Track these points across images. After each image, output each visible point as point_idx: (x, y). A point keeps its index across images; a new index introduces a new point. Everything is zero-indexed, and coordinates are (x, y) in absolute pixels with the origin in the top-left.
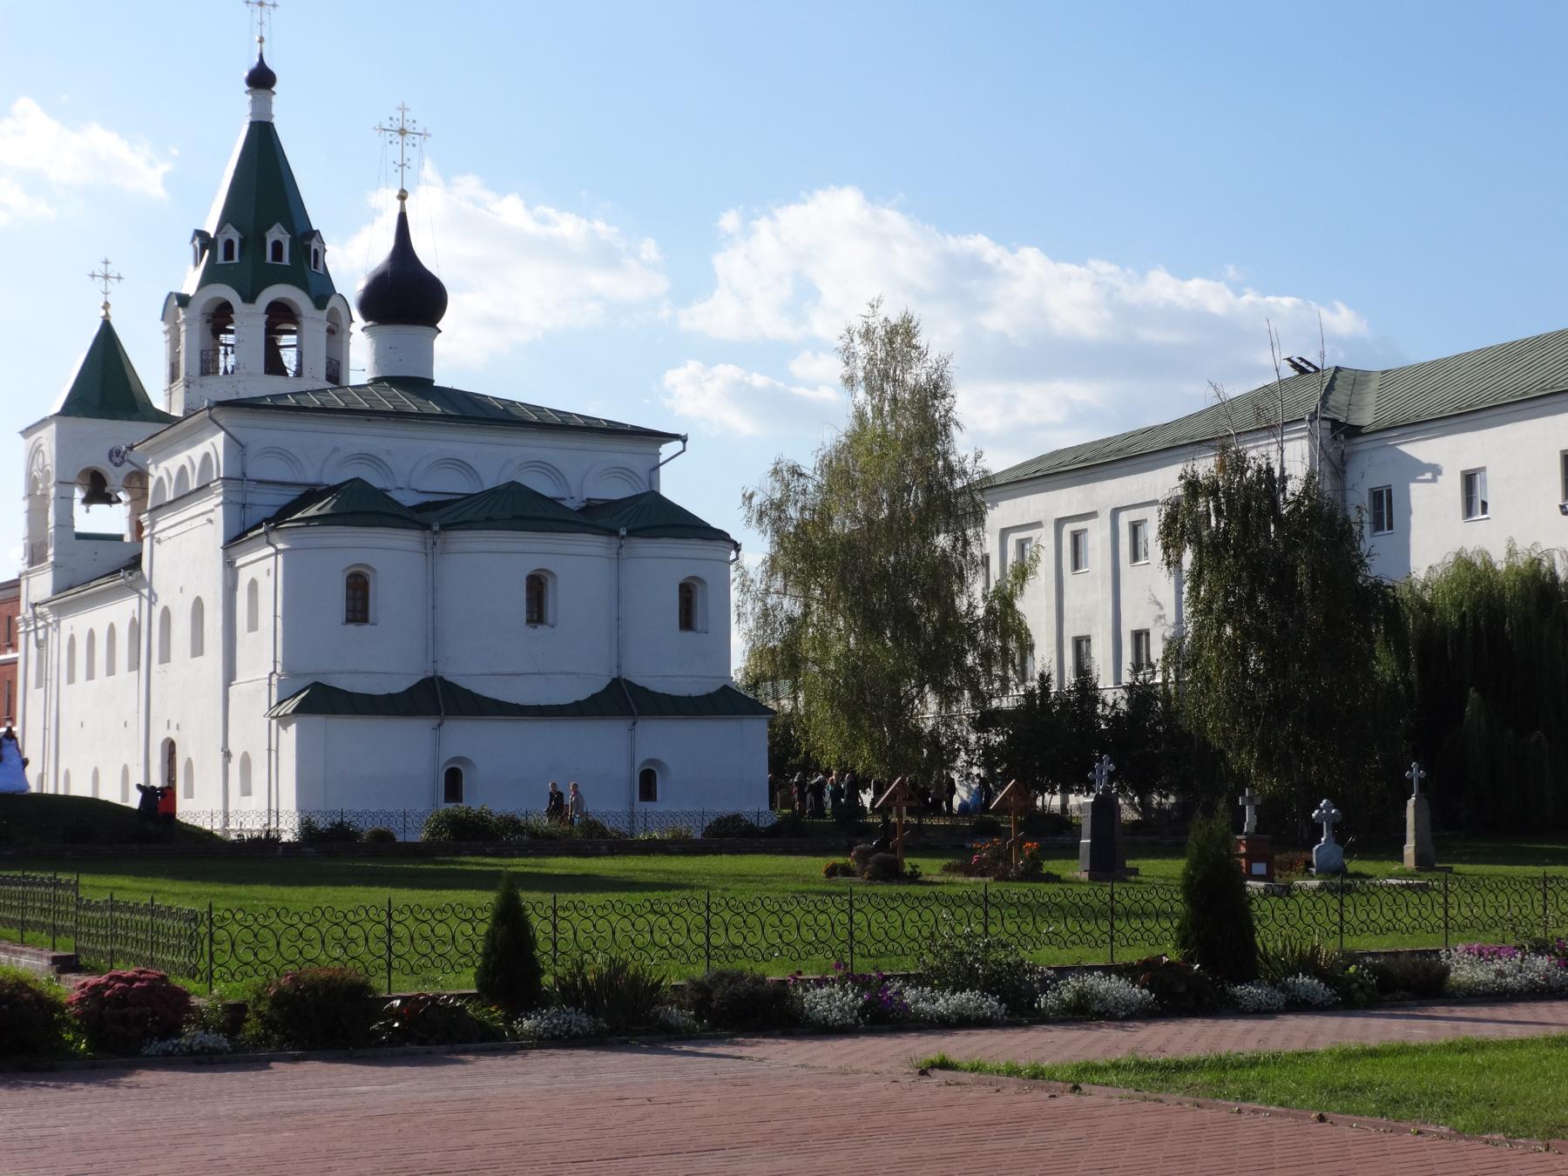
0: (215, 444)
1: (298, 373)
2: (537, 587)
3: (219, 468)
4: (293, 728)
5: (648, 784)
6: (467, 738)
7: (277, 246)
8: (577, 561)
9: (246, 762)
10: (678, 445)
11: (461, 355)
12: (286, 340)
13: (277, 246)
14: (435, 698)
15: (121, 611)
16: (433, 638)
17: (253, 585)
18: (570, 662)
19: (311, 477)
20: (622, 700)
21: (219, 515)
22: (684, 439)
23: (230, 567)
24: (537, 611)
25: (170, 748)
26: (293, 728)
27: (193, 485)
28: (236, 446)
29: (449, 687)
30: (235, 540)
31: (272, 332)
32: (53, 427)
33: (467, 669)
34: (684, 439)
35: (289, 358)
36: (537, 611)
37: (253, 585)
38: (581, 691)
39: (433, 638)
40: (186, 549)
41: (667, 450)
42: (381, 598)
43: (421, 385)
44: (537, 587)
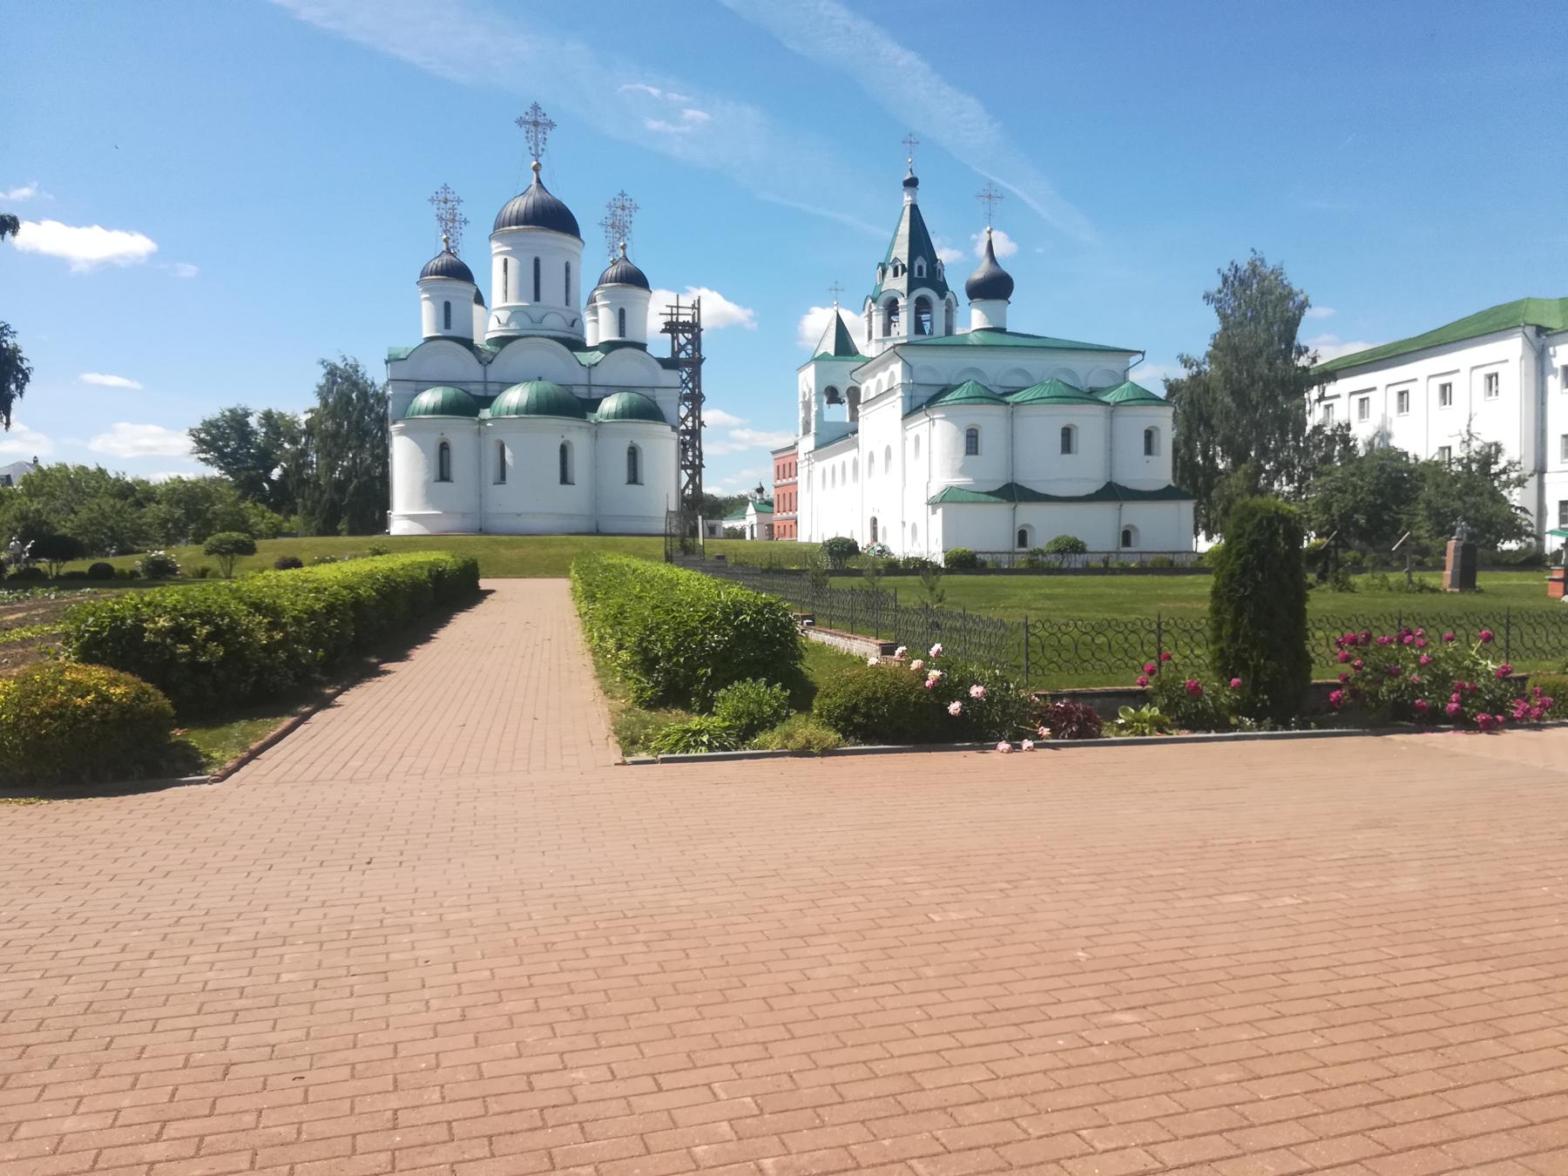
0: (897, 368)
1: (931, 333)
2: (1067, 433)
3: (899, 379)
4: (940, 511)
5: (1126, 537)
6: (1029, 514)
7: (920, 268)
8: (1087, 420)
9: (914, 527)
10: (1140, 357)
11: (1020, 315)
12: (924, 317)
13: (920, 268)
14: (1013, 493)
15: (848, 457)
16: (1012, 460)
17: (917, 439)
18: (1086, 471)
19: (944, 381)
20: (1112, 493)
21: (899, 402)
22: (1143, 353)
23: (904, 427)
24: (1067, 447)
25: (874, 521)
26: (940, 511)
27: (885, 389)
28: (909, 368)
29: (1021, 489)
30: (910, 412)
31: (918, 312)
32: (812, 368)
33: (1029, 478)
34: (1143, 353)
35: (927, 326)
36: (1067, 447)
37: (917, 439)
38: (1092, 488)
39: (1012, 460)
40: (881, 422)
41: (1134, 359)
42: (984, 441)
43: (1002, 331)
44: (1067, 433)
